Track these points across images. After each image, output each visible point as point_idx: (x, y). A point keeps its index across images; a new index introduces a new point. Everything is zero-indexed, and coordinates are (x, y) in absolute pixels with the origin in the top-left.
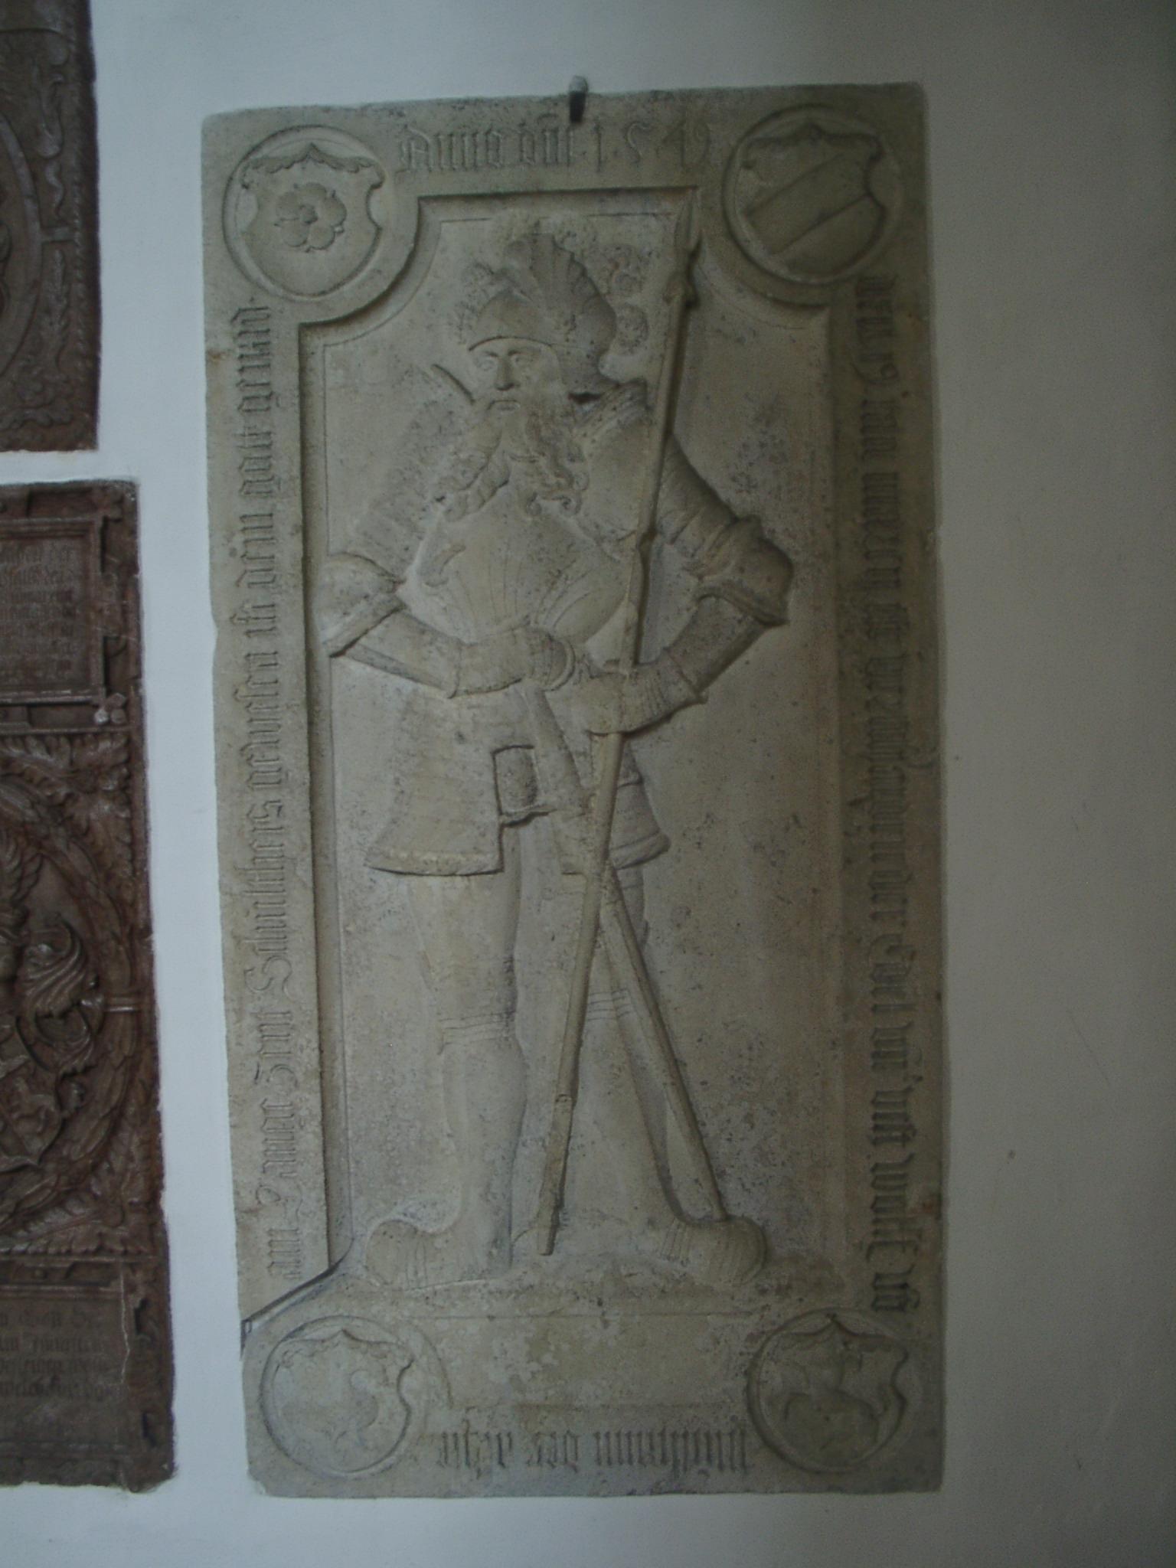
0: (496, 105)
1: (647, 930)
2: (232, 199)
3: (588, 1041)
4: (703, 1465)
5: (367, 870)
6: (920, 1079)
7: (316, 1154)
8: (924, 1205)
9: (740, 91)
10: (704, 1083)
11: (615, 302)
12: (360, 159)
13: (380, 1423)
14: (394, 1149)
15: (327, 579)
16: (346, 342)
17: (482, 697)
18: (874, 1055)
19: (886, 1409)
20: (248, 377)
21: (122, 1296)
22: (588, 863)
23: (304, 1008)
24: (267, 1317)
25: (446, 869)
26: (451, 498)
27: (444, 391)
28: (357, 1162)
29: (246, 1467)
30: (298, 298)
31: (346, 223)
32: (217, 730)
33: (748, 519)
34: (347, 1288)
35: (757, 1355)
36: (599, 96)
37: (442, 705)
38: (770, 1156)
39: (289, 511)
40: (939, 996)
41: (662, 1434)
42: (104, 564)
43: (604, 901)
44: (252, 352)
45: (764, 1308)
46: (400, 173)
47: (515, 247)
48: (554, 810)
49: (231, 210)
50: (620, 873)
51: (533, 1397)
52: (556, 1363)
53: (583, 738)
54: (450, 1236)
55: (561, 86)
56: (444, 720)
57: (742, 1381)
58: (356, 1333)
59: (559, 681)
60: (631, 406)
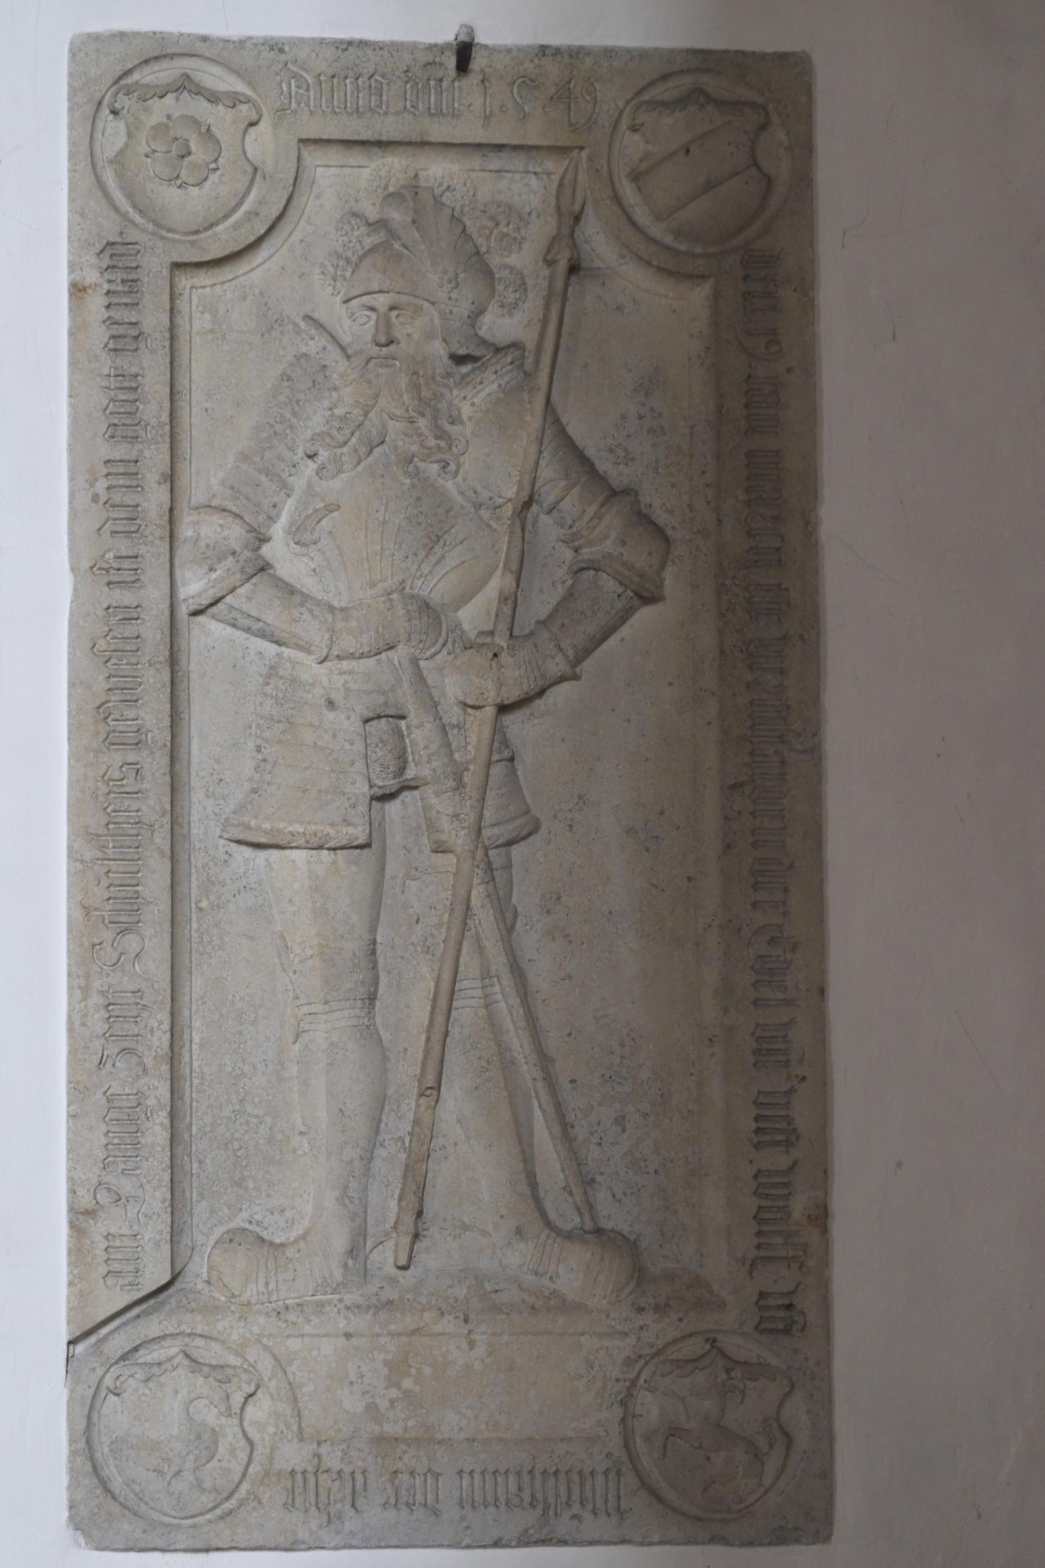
0: (381, 49)
1: (516, 915)
2: (100, 125)
3: (455, 1031)
4: (576, 1509)
5: (222, 841)
6: (804, 1078)
7: (164, 1149)
8: (809, 1216)
9: (628, 51)
10: (573, 1081)
11: (495, 261)
12: (237, 93)
13: (219, 1461)
14: (241, 1148)
15: (189, 533)
16: (213, 285)
17: (354, 663)
18: (757, 1052)
19: (771, 1447)
20: (117, 314)
22: (459, 838)
23: (156, 987)
24: (93, 1339)
25: (315, 842)
26: (324, 455)
27: (315, 345)
28: (200, 1162)
29: (66, 1514)
30: (170, 235)
31: (221, 161)
32: (72, 685)
33: (625, 492)
34: (189, 1303)
35: (634, 1383)
36: (486, 47)
37: (309, 668)
38: (642, 1164)
39: (156, 458)
40: (822, 992)
43: (476, 881)
44: (120, 288)
45: (641, 1328)
46: (281, 113)
47: (394, 198)
48: (426, 784)
49: (98, 136)
50: (491, 853)
51: (388, 1428)
52: (417, 1389)
53: (457, 709)
54: (302, 1245)
55: (447, 35)
56: (312, 685)
57: (618, 1411)
58: (195, 1354)
59: (433, 650)
60: (511, 371)
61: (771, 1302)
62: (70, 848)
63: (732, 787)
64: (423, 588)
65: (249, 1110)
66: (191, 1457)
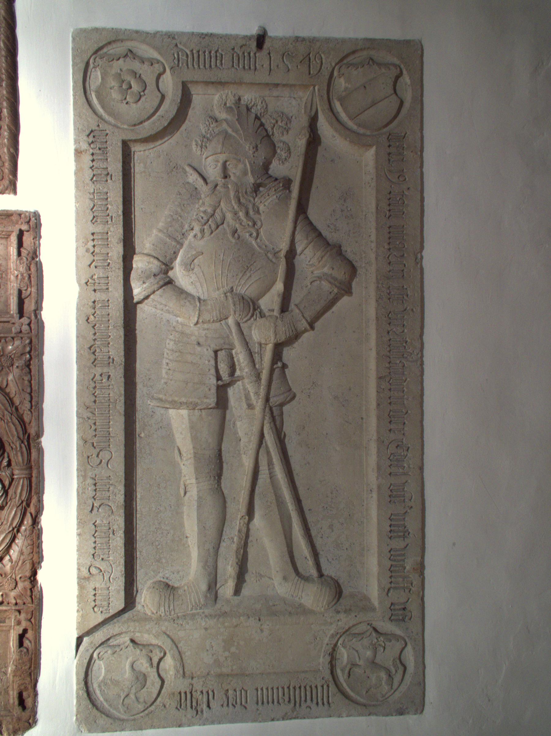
0: (221, 38)
6: (411, 507)
7: (121, 548)
8: (414, 568)
9: (336, 39)
10: (310, 510)
11: (276, 139)
14: (159, 545)
16: (145, 150)
19: (396, 671)
21: (12, 627)
22: (259, 404)
23: (117, 475)
31: (146, 92)
33: (334, 246)
34: (133, 617)
38: (341, 545)
41: (289, 688)
42: (19, 254)
51: (225, 670)
52: (237, 652)
60: (281, 190)
61: (397, 607)
62: (77, 412)
63: (380, 378)
64: (241, 290)
65: (163, 527)
66: (134, 688)
